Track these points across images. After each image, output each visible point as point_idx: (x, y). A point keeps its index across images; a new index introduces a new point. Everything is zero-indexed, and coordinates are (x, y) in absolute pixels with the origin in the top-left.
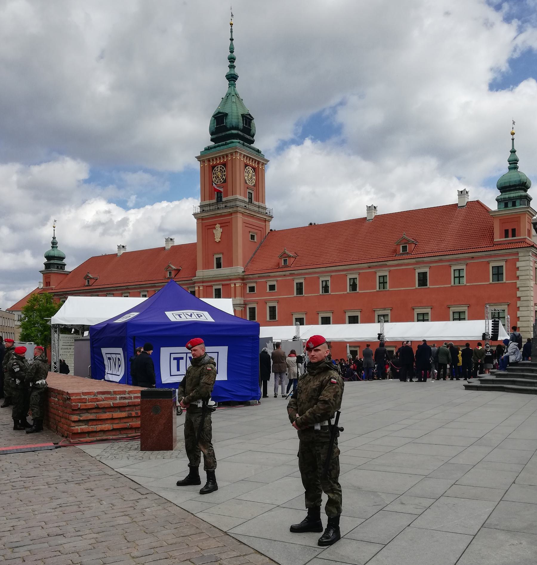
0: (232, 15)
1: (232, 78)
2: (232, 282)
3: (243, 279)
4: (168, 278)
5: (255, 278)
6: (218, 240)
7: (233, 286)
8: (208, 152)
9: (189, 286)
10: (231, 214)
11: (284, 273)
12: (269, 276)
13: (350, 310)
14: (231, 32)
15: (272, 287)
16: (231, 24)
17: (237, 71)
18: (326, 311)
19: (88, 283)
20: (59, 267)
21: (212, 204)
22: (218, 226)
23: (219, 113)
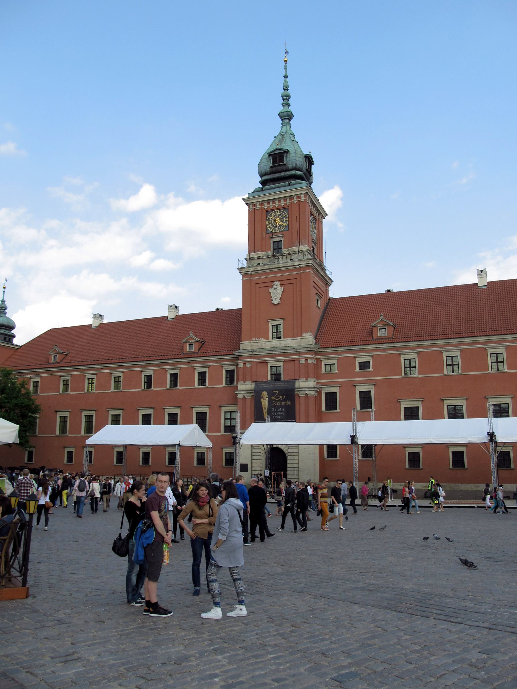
0: (287, 52)
1: (286, 117)
2: (301, 356)
3: (316, 353)
4: (187, 353)
5: (336, 353)
6: (276, 302)
7: (302, 362)
8: (261, 193)
9: (223, 363)
10: (300, 268)
11: (385, 346)
12: (360, 351)
13: (495, 396)
14: (286, 69)
15: (364, 365)
16: (286, 61)
17: (291, 109)
18: (456, 397)
19: (55, 359)
20: (7, 339)
21: (268, 257)
22: (277, 283)
23: (277, 149)
